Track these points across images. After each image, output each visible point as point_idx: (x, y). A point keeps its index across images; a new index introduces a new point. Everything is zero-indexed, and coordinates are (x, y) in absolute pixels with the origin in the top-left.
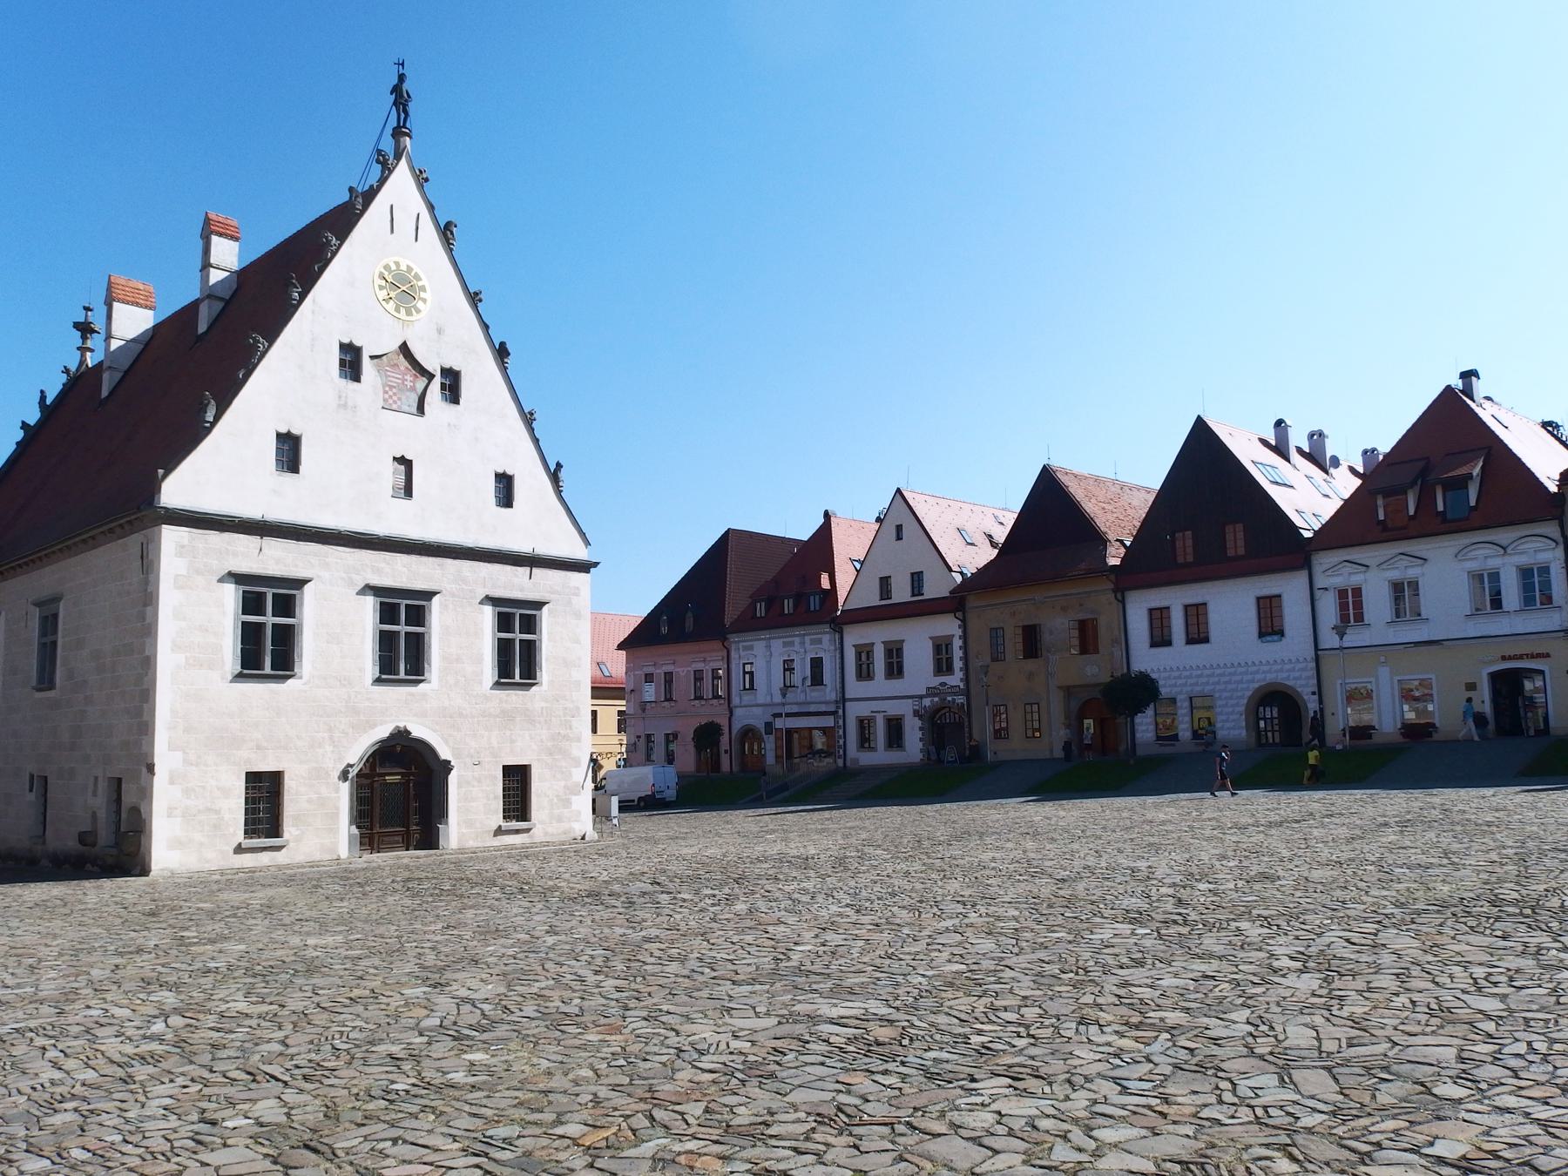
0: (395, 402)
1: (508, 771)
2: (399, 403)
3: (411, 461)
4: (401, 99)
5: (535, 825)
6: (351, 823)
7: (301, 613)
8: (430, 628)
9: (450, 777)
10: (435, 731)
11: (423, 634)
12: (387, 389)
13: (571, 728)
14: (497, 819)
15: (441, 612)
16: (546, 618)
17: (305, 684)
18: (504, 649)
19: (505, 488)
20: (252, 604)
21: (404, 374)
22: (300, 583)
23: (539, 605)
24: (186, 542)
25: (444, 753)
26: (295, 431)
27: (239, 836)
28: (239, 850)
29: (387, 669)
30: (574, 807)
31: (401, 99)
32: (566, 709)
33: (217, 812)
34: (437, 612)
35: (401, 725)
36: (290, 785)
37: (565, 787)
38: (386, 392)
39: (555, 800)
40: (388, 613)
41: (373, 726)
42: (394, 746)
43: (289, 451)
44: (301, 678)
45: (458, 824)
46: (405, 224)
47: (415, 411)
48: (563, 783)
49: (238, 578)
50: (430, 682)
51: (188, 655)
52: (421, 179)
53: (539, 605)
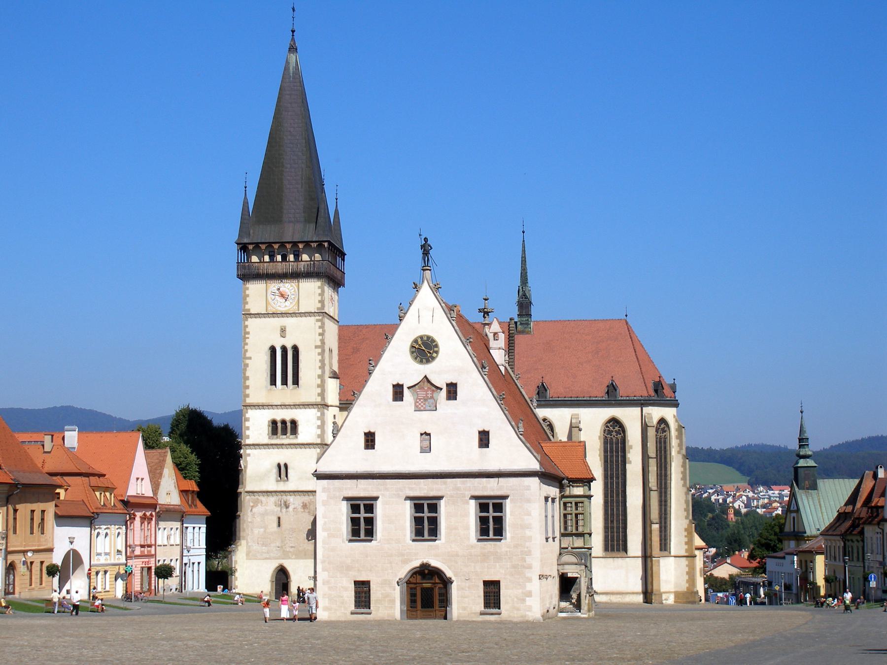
0: (422, 406)
1: (486, 583)
2: (424, 406)
3: (430, 434)
4: (426, 249)
5: (501, 611)
6: (401, 604)
7: (376, 512)
8: (440, 513)
9: (452, 585)
10: (444, 563)
11: (437, 517)
12: (418, 400)
13: (525, 561)
14: (480, 606)
15: (446, 506)
16: (508, 505)
17: (378, 543)
18: (483, 521)
19: (484, 439)
20: (355, 508)
21: (427, 391)
22: (376, 498)
23: (505, 497)
24: (326, 486)
25: (449, 573)
26: (372, 431)
27: (352, 607)
28: (352, 613)
29: (418, 533)
30: (528, 603)
31: (426, 249)
32: (522, 551)
33: (342, 597)
34: (443, 506)
35: (425, 561)
36: (373, 586)
37: (522, 593)
38: (416, 402)
39: (515, 599)
40: (418, 508)
41: (412, 561)
42: (424, 570)
43: (370, 440)
44: (376, 540)
45: (458, 608)
46: (426, 315)
47: (435, 409)
48: (520, 591)
49: (347, 499)
50: (440, 540)
51: (328, 532)
52: (436, 289)
53: (505, 497)
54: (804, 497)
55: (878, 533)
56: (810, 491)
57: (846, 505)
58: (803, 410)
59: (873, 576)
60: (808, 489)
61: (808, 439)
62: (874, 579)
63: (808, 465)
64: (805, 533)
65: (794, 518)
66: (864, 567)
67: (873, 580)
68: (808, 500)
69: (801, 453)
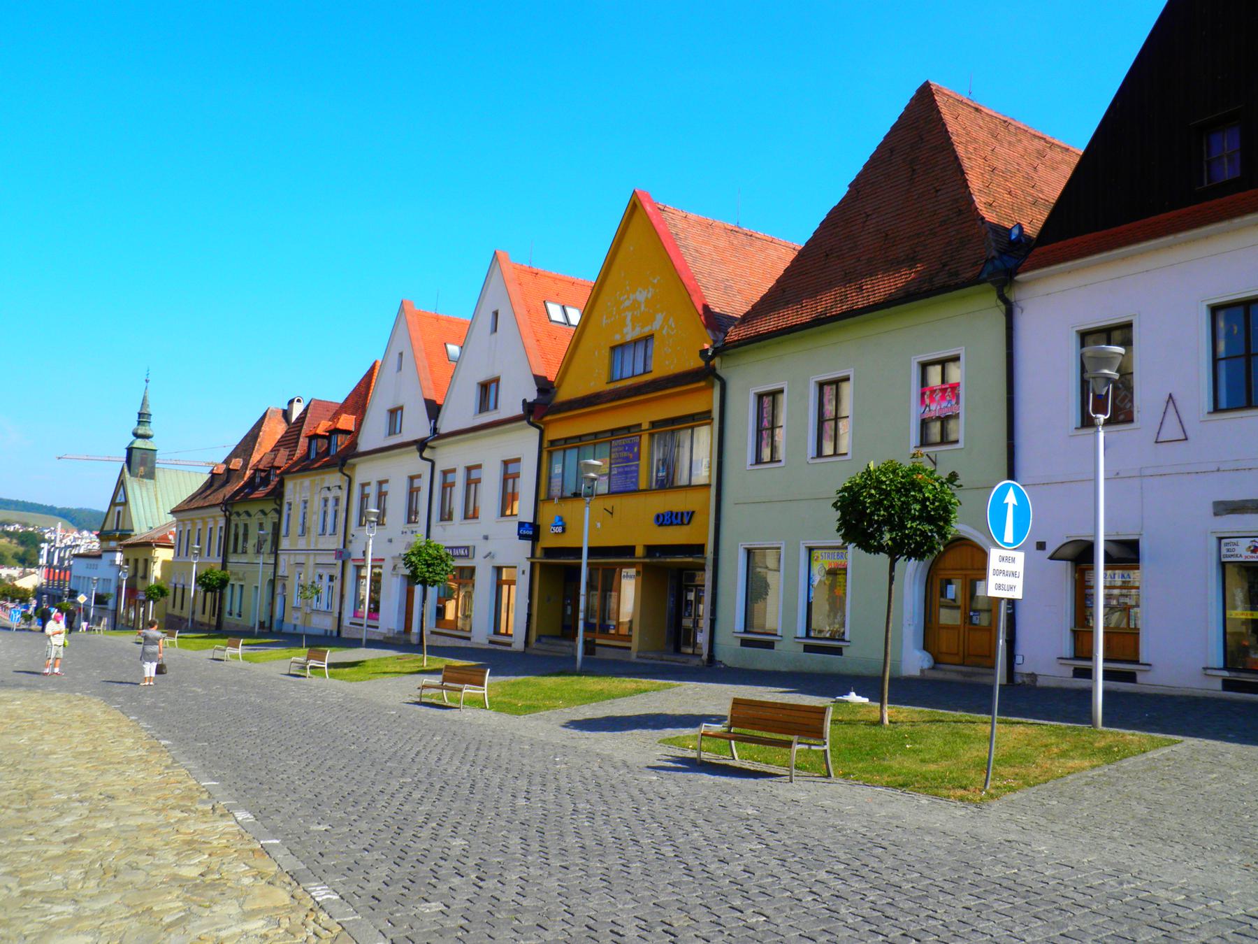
54: (136, 487)
55: (329, 489)
56: (145, 480)
57: (234, 454)
58: (150, 378)
59: (1011, 499)
60: (142, 477)
61: (150, 415)
62: (1018, 534)
63: (147, 447)
64: (133, 530)
65: (119, 513)
66: (276, 565)
67: (1009, 536)
68: (141, 492)
69: (140, 432)
